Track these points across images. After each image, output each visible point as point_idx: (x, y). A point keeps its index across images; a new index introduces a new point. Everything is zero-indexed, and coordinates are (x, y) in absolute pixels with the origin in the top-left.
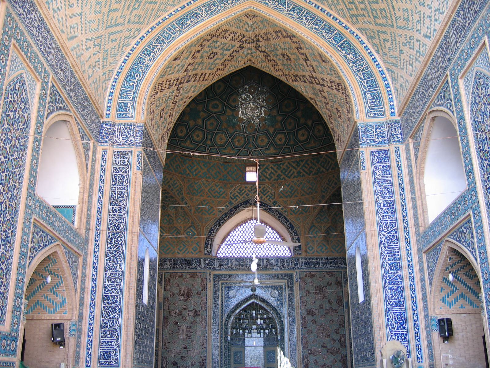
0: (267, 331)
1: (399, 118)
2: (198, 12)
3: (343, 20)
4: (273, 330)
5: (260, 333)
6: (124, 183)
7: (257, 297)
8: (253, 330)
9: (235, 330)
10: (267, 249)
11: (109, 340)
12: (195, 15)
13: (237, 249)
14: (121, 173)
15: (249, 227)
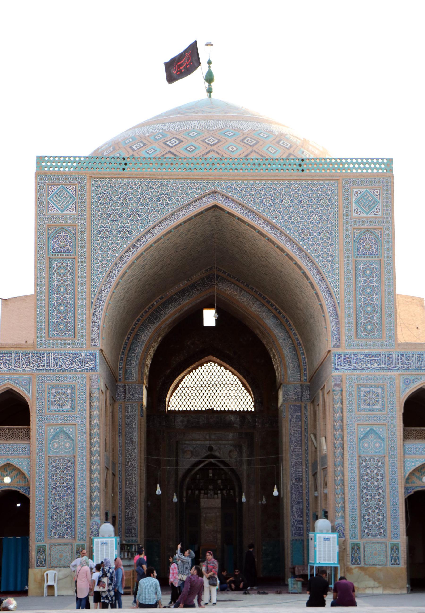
0: (225, 492)
1: (309, 384)
2: (176, 297)
3: (277, 307)
4: (232, 491)
5: (217, 494)
6: (134, 426)
7: (214, 457)
8: (210, 490)
9: (190, 491)
10: (226, 397)
11: (131, 522)
12: (174, 300)
13: (192, 397)
14: (131, 419)
15: (205, 371)
